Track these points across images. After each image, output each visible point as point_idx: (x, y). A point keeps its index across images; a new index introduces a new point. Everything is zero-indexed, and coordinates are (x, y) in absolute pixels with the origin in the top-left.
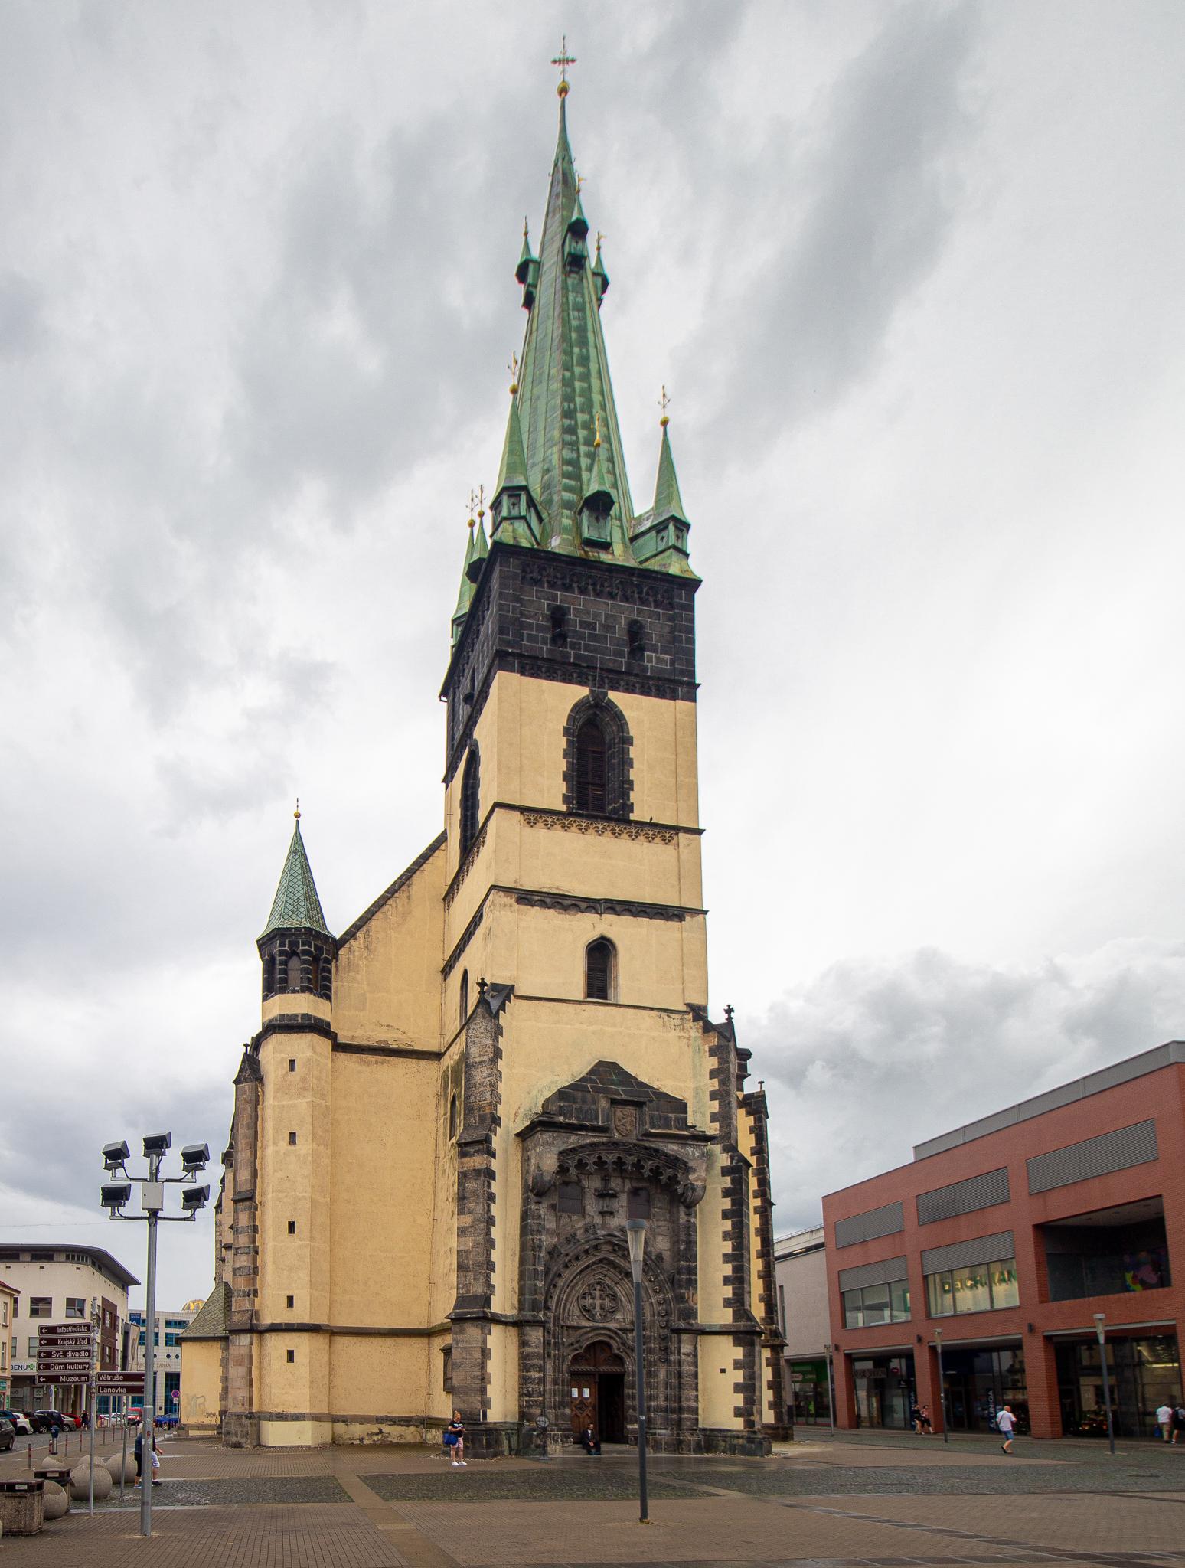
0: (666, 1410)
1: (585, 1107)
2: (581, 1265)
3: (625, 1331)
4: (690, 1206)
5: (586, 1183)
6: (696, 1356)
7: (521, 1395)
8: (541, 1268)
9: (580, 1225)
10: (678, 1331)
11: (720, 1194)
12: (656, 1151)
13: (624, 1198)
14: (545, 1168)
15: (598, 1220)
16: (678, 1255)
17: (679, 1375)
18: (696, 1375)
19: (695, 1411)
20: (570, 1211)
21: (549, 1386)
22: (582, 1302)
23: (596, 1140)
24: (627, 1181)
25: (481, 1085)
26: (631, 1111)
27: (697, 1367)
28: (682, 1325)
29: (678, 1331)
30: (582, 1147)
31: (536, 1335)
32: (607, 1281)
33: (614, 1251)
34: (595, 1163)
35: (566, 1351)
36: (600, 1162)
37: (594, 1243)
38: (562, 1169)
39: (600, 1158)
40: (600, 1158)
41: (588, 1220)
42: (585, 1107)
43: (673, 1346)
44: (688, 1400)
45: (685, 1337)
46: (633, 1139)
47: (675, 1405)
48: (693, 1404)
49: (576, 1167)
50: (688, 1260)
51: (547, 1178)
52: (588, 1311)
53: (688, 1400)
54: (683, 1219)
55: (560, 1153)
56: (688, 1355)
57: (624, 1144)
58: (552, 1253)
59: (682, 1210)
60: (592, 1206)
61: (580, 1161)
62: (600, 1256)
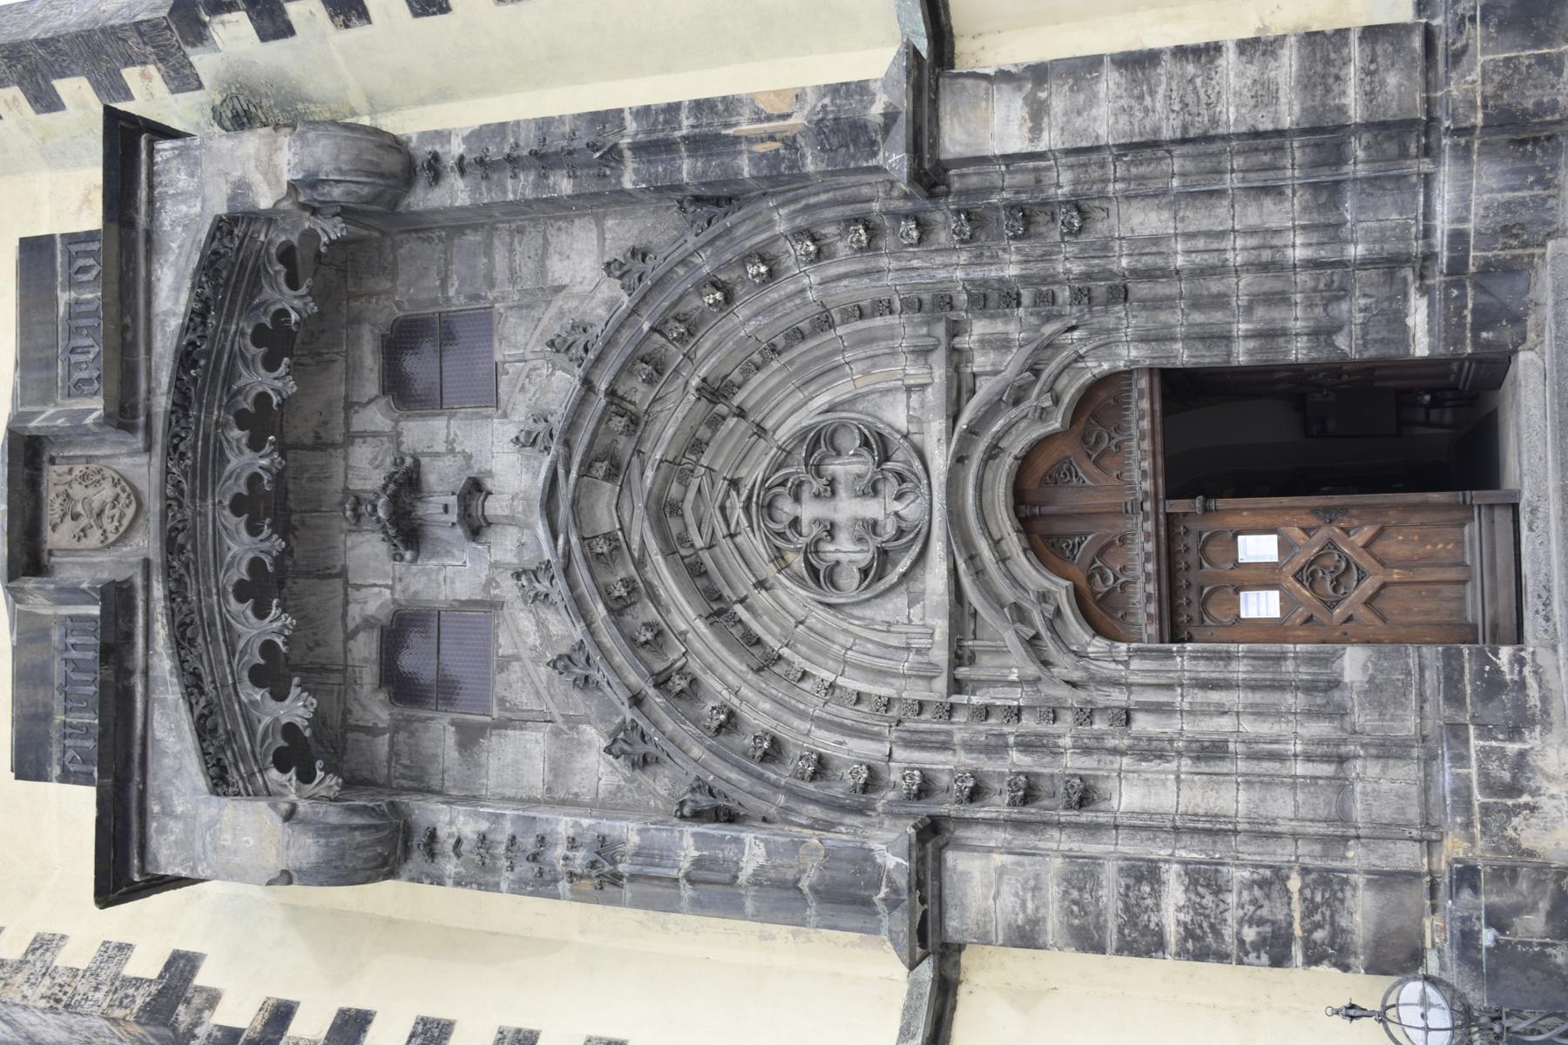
0: (1328, 192)
1: (57, 670)
2: (684, 612)
3: (958, 392)
4: (401, 167)
5: (374, 602)
6: (1039, 73)
7: (1280, 960)
8: (687, 843)
9: (526, 622)
10: (930, 176)
11: (358, 32)
12: (186, 358)
13: (425, 434)
14: (274, 862)
15: (505, 547)
16: (601, 200)
17: (1145, 147)
18: (1138, 63)
19: (1321, 46)
20: (487, 661)
21: (1232, 801)
22: (849, 579)
23: (161, 631)
24: (361, 421)
25: (71, 1031)
26: (53, 475)
27: (1093, 63)
28: (895, 159)
29: (930, 176)
30: (193, 684)
31: (982, 878)
32: (753, 473)
33: (615, 471)
34: (261, 613)
35: (1065, 667)
36: (260, 588)
37: (581, 572)
38: (296, 754)
39: (242, 591)
40: (242, 591)
41: (508, 589)
42: (57, 670)
43: (1007, 188)
44: (1264, 94)
45: (955, 139)
46: (142, 468)
47: (1294, 163)
48: (1288, 64)
49: (280, 696)
50: (613, 155)
51: (307, 849)
52: (884, 557)
53: (1264, 94)
54: (457, 193)
55: (220, 781)
56: (1038, 113)
57: (173, 501)
58: (633, 749)
59: (424, 199)
60: (454, 574)
61: (258, 677)
62: (641, 532)
